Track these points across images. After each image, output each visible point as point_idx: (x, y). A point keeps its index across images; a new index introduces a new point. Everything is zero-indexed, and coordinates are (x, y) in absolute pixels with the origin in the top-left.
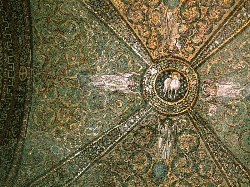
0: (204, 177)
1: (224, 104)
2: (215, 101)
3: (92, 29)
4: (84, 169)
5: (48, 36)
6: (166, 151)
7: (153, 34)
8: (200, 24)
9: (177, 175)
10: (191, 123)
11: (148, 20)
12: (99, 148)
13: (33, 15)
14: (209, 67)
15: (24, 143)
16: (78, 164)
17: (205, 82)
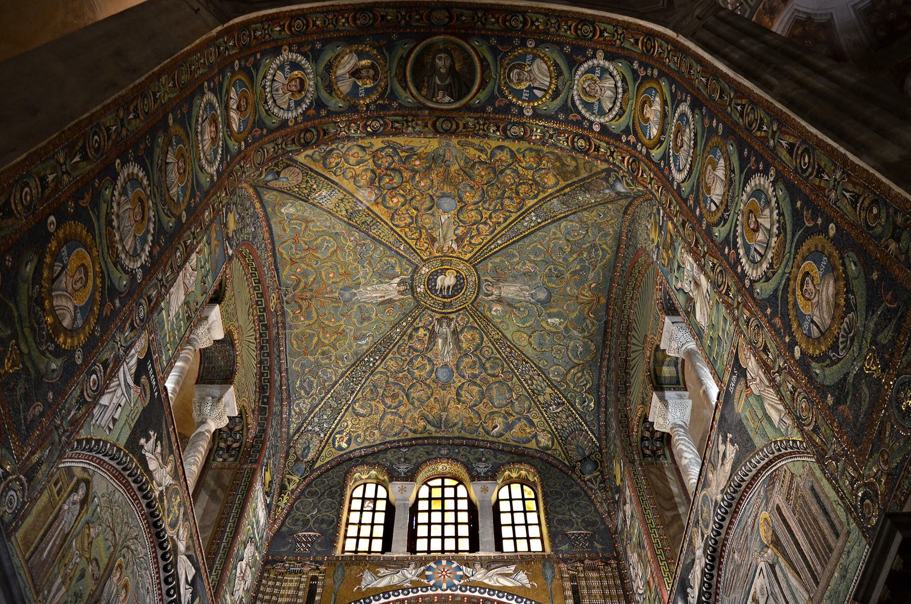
0: (493, 376)
1: (510, 304)
2: (500, 300)
3: (351, 241)
5: (298, 256)
6: (448, 352)
7: (423, 236)
8: (481, 226)
9: (463, 377)
10: (471, 320)
11: (416, 222)
12: (372, 359)
13: (276, 239)
14: (490, 265)
15: (287, 373)
17: (486, 280)
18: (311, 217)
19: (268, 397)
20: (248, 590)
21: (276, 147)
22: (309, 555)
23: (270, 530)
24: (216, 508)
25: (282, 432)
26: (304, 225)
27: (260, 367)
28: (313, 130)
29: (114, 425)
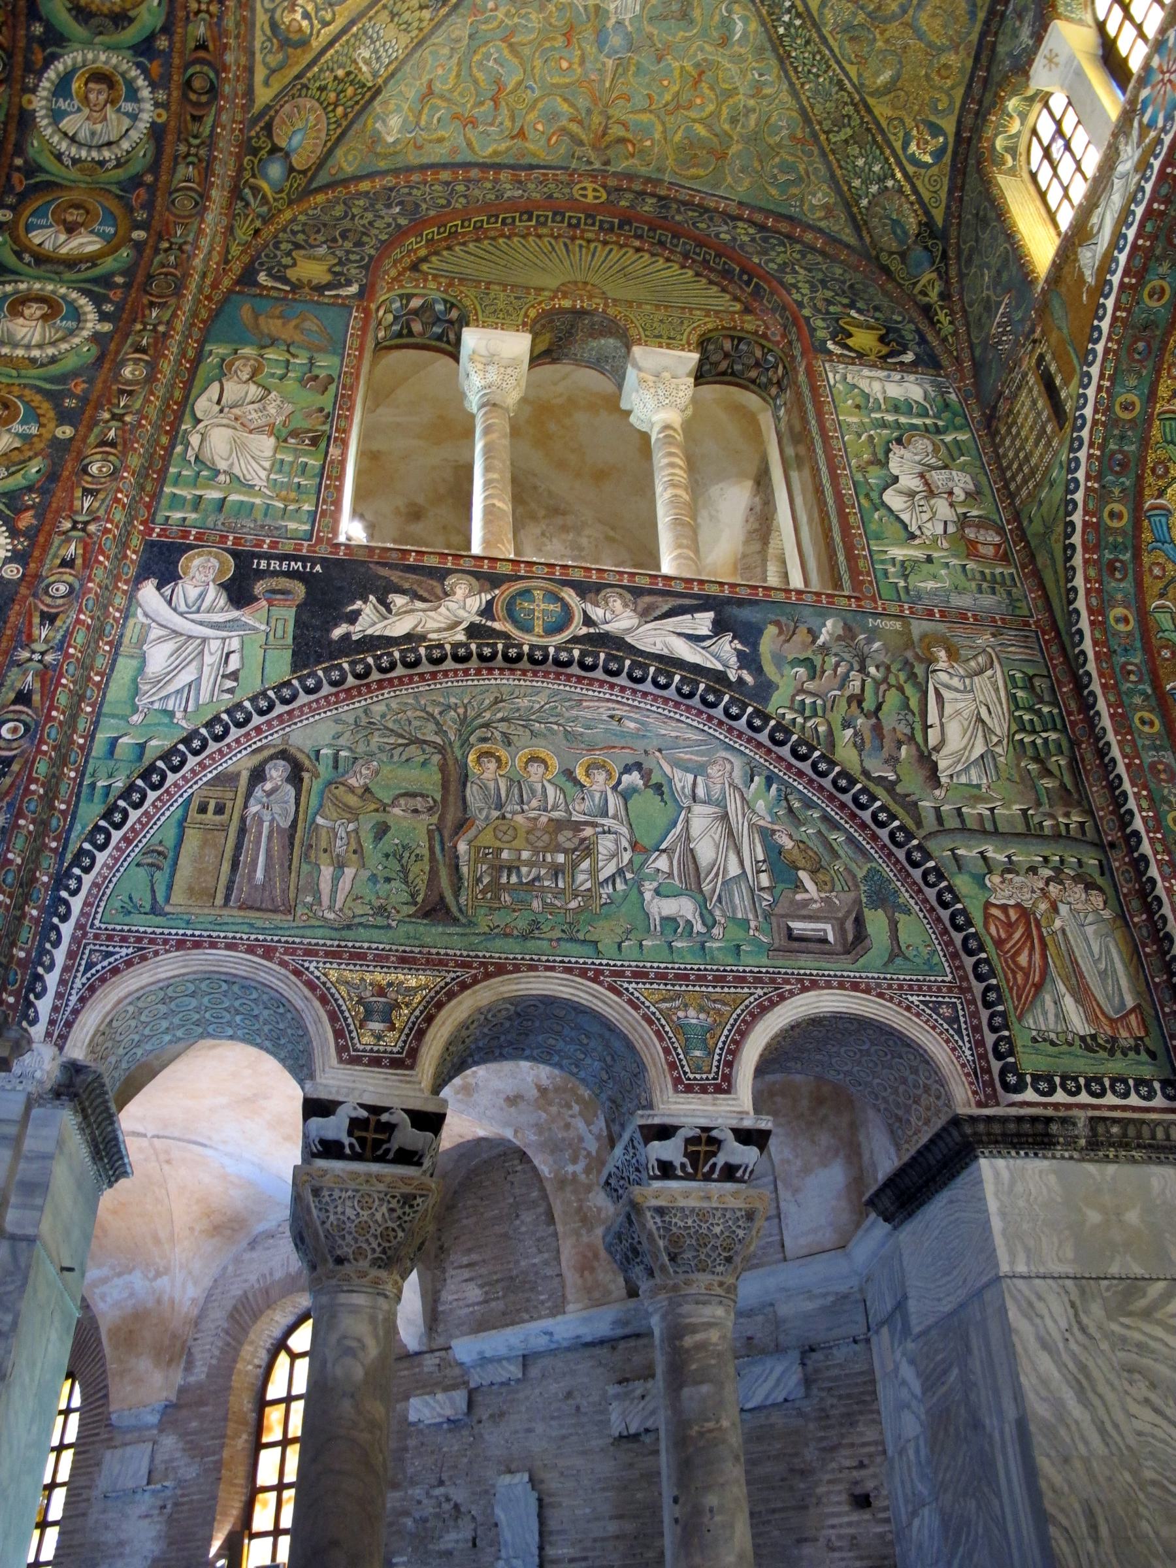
3: (496, 9)
4: (832, 62)
5: (508, 123)
12: (786, 18)
13: (459, 159)
16: (818, 76)
18: (420, 84)
19: (743, 271)
20: (973, 496)
21: (190, 159)
22: (1017, 342)
23: (962, 380)
24: (807, 472)
25: (842, 262)
26: (439, 102)
27: (694, 261)
28: (190, 71)
29: (236, 680)
